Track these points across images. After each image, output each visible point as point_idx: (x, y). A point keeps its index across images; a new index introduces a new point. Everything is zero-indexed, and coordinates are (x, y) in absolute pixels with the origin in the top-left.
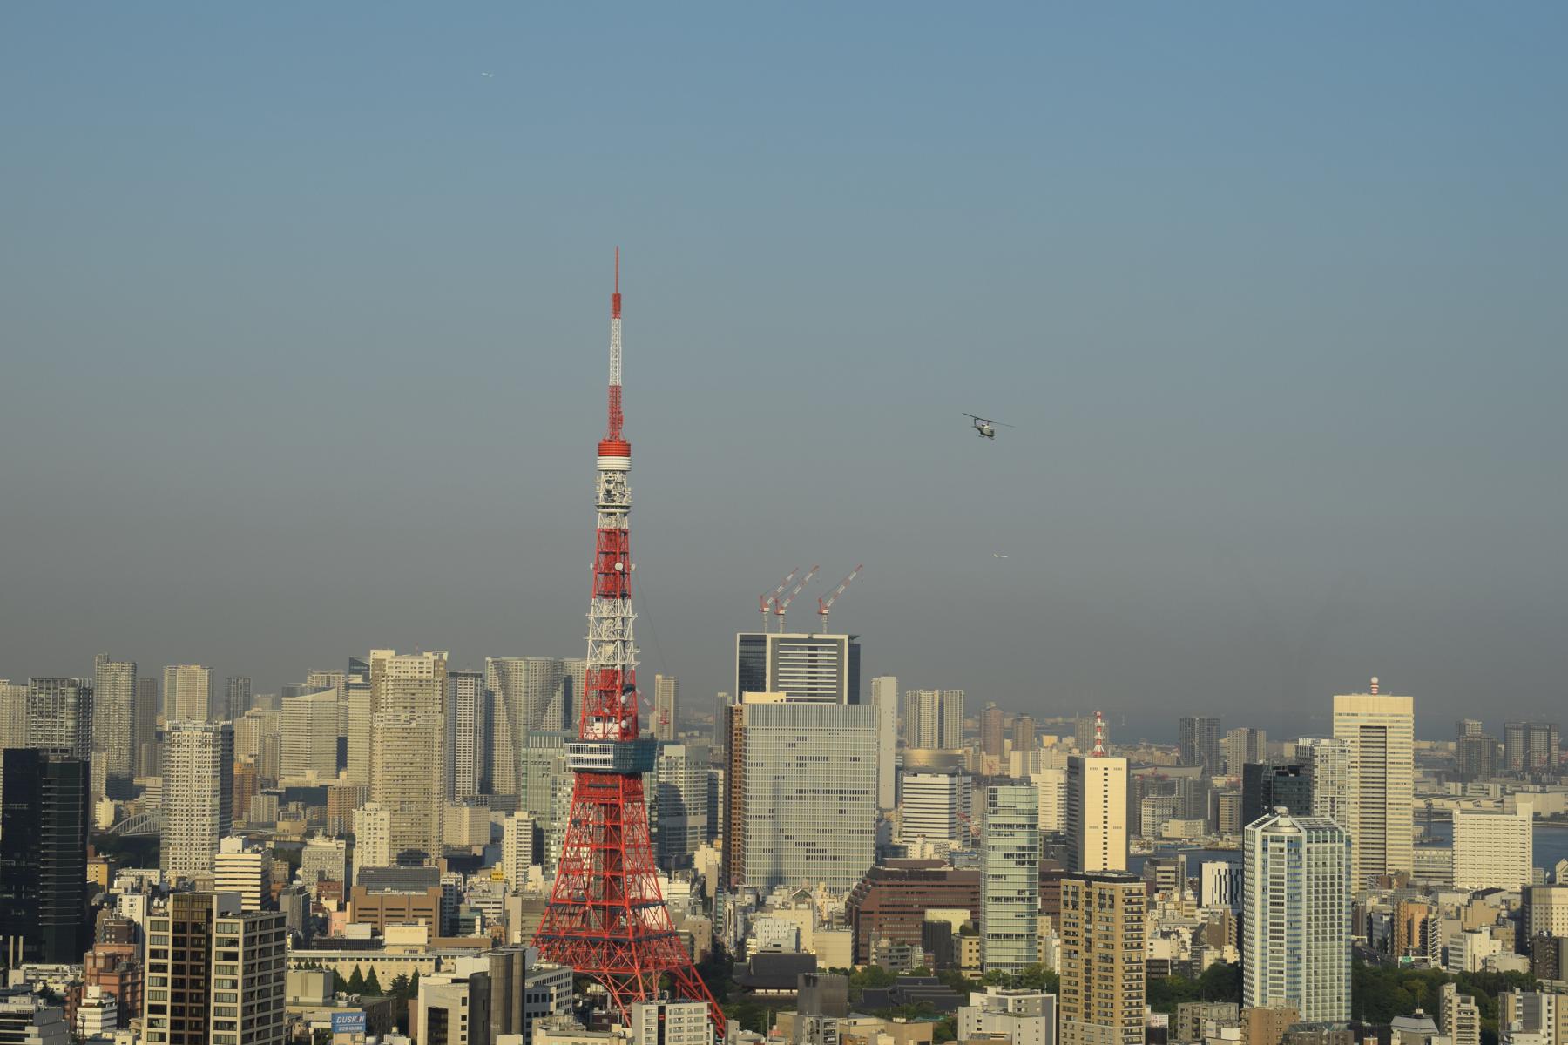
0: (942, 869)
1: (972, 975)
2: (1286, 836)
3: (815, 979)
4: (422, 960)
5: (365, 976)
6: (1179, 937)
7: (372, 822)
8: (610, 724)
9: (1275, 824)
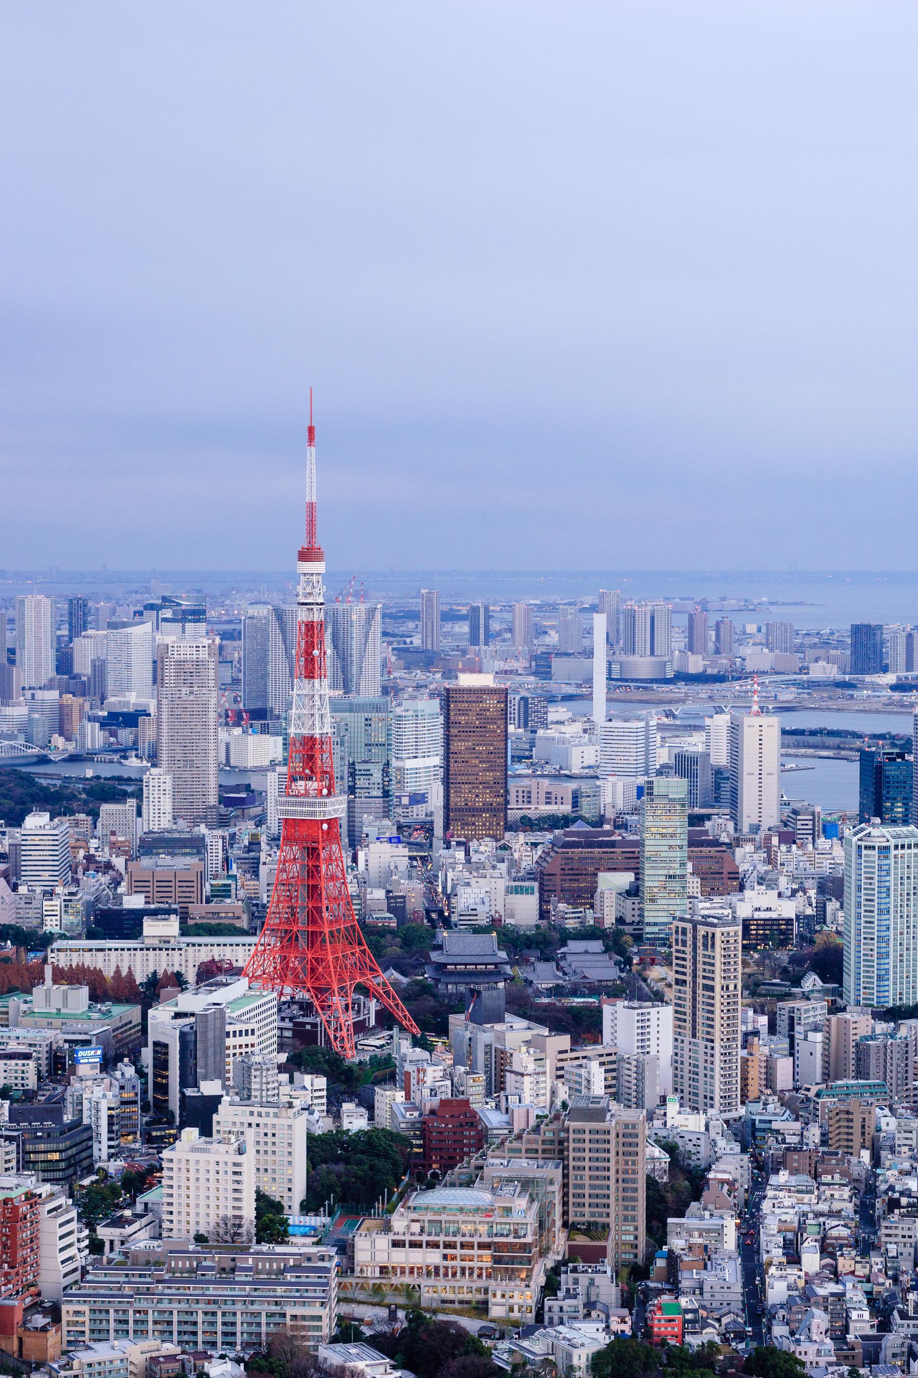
0: (613, 838)
1: (634, 929)
2: (877, 845)
3: (479, 993)
4: (173, 949)
5: (124, 973)
6: (805, 894)
7: (157, 785)
8: (311, 783)
9: (869, 835)
